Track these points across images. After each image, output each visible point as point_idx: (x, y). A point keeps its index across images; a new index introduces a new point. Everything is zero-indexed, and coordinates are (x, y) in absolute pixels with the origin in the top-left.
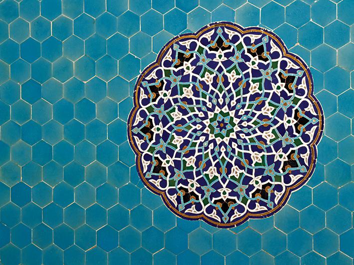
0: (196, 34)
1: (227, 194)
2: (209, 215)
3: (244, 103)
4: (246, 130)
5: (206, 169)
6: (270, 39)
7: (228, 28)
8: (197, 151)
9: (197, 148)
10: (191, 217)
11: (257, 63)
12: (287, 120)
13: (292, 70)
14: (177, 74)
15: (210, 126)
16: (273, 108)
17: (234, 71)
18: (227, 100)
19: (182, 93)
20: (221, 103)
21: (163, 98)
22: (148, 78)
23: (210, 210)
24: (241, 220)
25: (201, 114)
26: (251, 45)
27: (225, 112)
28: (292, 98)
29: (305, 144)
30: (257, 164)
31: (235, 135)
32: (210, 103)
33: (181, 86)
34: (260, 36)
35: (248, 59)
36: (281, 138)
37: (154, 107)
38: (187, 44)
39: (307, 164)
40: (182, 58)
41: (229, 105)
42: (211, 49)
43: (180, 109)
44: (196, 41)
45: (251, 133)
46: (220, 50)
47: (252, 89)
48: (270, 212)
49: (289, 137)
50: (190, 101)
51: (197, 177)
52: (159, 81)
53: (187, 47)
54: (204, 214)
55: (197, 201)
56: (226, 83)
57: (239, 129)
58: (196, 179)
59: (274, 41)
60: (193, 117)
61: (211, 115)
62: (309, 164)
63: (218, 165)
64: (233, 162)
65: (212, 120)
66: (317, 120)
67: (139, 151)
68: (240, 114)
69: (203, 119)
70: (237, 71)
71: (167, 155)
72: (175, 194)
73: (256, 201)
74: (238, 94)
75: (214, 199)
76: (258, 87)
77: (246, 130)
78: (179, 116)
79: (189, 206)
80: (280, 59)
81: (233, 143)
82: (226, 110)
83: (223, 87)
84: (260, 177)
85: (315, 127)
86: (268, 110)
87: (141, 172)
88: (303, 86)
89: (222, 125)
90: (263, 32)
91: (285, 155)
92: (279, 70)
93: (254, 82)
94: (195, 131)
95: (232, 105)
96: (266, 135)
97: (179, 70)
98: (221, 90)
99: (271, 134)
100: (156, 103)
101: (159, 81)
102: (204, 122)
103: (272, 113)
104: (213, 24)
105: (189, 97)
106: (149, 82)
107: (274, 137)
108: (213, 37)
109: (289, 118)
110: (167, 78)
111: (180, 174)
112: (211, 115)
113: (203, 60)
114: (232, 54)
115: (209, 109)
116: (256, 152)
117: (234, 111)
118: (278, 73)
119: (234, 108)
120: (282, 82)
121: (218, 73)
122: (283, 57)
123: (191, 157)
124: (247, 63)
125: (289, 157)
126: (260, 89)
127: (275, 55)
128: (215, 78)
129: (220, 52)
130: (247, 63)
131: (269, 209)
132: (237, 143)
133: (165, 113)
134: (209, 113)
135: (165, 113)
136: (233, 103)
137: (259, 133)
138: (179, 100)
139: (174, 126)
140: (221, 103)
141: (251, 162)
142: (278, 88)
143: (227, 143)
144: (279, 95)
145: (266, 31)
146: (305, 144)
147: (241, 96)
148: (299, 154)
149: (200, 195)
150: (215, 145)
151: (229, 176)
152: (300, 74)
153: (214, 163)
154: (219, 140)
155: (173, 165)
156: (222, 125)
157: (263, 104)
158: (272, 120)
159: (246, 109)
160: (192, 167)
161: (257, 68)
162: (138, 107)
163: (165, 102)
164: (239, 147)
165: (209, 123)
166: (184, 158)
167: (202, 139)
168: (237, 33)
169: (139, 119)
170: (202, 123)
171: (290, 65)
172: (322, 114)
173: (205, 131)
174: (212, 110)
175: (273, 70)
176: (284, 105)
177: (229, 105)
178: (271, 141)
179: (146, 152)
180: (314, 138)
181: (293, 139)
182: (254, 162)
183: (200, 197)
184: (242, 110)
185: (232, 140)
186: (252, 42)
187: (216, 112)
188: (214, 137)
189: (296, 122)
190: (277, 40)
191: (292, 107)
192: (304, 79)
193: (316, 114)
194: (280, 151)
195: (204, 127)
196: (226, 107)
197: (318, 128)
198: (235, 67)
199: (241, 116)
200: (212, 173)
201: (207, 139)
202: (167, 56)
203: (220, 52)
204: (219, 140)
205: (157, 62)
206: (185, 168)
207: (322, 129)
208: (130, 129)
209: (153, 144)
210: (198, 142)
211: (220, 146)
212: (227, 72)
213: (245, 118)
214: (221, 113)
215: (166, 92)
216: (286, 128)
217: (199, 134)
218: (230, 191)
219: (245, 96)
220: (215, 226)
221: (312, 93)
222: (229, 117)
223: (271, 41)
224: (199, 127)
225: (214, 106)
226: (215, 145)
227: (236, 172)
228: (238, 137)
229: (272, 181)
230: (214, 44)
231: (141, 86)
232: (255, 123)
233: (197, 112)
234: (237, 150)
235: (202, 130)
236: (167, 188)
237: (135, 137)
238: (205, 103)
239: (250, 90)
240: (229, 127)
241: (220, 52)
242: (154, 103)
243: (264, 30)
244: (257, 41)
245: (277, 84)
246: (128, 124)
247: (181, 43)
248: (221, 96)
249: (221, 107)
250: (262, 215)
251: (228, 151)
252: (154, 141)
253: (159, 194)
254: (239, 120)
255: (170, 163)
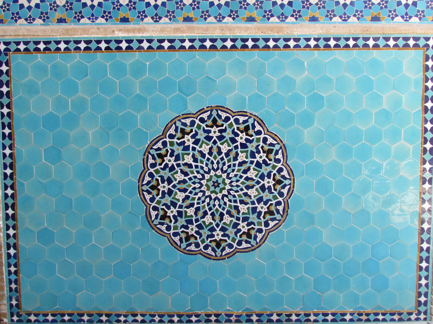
0: (195, 114)
1: (220, 236)
2: (205, 251)
3: (234, 168)
4: (235, 189)
5: (203, 217)
6: (255, 120)
7: (221, 110)
8: (196, 204)
9: (196, 202)
10: (192, 253)
11: (244, 138)
12: (267, 181)
13: (271, 145)
14: (179, 144)
15: (207, 185)
16: (257, 172)
17: (226, 143)
18: (220, 166)
19: (183, 159)
20: (215, 168)
21: (168, 163)
22: (155, 147)
23: (206, 247)
24: (231, 254)
25: (199, 176)
26: (240, 124)
27: (219, 174)
28: (271, 165)
29: (280, 199)
30: (243, 213)
31: (226, 192)
32: (207, 168)
33: (183, 154)
34: (247, 118)
35: (237, 135)
36: (262, 194)
37: (160, 170)
38: (188, 121)
39: (282, 213)
40: (183, 132)
41: (222, 169)
42: (207, 126)
43: (182, 172)
44: (195, 119)
45: (239, 191)
46: (215, 127)
47: (240, 157)
48: (253, 248)
49: (268, 194)
50: (190, 166)
51: (196, 223)
52: (165, 149)
53: (187, 124)
54: (202, 251)
55: (196, 241)
56: (220, 153)
57: (230, 188)
58: (195, 224)
59: (258, 122)
60: (193, 178)
61: (207, 176)
62: (283, 213)
63: (213, 215)
64: (225, 212)
65: (208, 181)
66: (290, 182)
67: (148, 203)
68: (230, 176)
69: (201, 179)
70: (228, 144)
71: (172, 207)
72: (178, 236)
73: (242, 240)
74: (229, 161)
75: (209, 239)
76: (244, 156)
77: (235, 189)
78: (181, 177)
79: (190, 245)
80: (262, 136)
81: (225, 198)
82: (219, 173)
83: (217, 155)
84: (246, 223)
85: (288, 187)
86: (253, 173)
87: (149, 219)
88: (279, 156)
89: (216, 184)
90: (248, 114)
91: (265, 207)
92: (261, 144)
93: (242, 152)
94: (194, 188)
95: (224, 169)
96: (251, 192)
97: (181, 142)
98: (215, 158)
99: (255, 191)
100: (162, 166)
101: (165, 149)
102: (202, 182)
103: (256, 176)
104: (209, 107)
105: (189, 163)
106: (156, 150)
107: (257, 193)
108: (209, 117)
109: (269, 180)
110: (172, 148)
111: (182, 221)
112: (207, 176)
113: (201, 135)
114: (225, 130)
115: (205, 172)
116: (243, 205)
117: (226, 174)
118: (261, 146)
119: (226, 171)
120: (263, 153)
121: (213, 145)
122: (265, 134)
123: (191, 208)
124: (236, 138)
125: (268, 208)
126: (247, 157)
127: (259, 133)
128: (211, 149)
129: (215, 129)
130: (236, 138)
131: (253, 246)
132: (228, 198)
133: (169, 175)
134: (206, 175)
135: (169, 175)
136: (225, 168)
137: (245, 191)
138: (181, 165)
139: (177, 185)
140: (215, 168)
141: (239, 212)
142: (261, 157)
143: (220, 198)
144: (261, 162)
145: (252, 114)
146: (280, 199)
147: (232, 163)
148: (276, 206)
149: (198, 237)
150: (211, 199)
151: (222, 222)
152: (277, 147)
153: (209, 213)
154: (214, 195)
155: (176, 214)
156: (216, 184)
157: (249, 169)
158: (255, 181)
159: (235, 173)
160: (191, 216)
161: (245, 142)
162: (146, 169)
163: (170, 166)
164: (230, 201)
165: (206, 183)
166: (186, 209)
167: (200, 195)
168: (228, 115)
169: (147, 179)
170: (200, 183)
171: (270, 140)
172: (294, 177)
173: (202, 189)
174: (208, 173)
175: (257, 144)
176: (265, 170)
177: (222, 169)
178: (255, 196)
179: (154, 204)
180: (287, 194)
181: (271, 195)
182: (241, 212)
183: (198, 238)
184: (232, 173)
185: (224, 196)
186: (241, 122)
187: (211, 174)
188: (210, 194)
189: (274, 182)
190: (260, 122)
191: (271, 172)
192: (281, 151)
193: (289, 177)
194: (262, 204)
195: (202, 185)
196: (220, 171)
197: (290, 188)
198: (227, 141)
199: (231, 178)
200: (208, 220)
201: (204, 195)
202: (171, 130)
203: (215, 129)
204: (213, 196)
205: (162, 135)
206: (186, 216)
207: (293, 188)
208: (140, 186)
209: (160, 198)
210: (197, 197)
211: (215, 200)
212: (220, 144)
213: (234, 179)
214: (216, 175)
215: (170, 158)
216: (266, 187)
217: (197, 191)
218: (222, 233)
219: (235, 163)
220: (211, 259)
221: (286, 162)
222: (221, 179)
223: (256, 122)
224: (197, 185)
225: (209, 170)
226: (211, 199)
227: (227, 219)
228: (229, 193)
229: (255, 225)
230: (210, 123)
231: (149, 153)
232: (243, 183)
233: (196, 174)
234: (228, 203)
235: (200, 188)
236: (172, 231)
237: (145, 193)
238: (202, 168)
239: (238, 158)
240: (221, 186)
241: (215, 129)
242: (160, 167)
243: (250, 114)
244: (244, 122)
245: (260, 155)
246: (139, 182)
247: (182, 120)
248: (215, 162)
249: (216, 170)
250: (246, 250)
251: (221, 203)
252: (160, 196)
253: (165, 236)
254: (229, 181)
255: (174, 213)
